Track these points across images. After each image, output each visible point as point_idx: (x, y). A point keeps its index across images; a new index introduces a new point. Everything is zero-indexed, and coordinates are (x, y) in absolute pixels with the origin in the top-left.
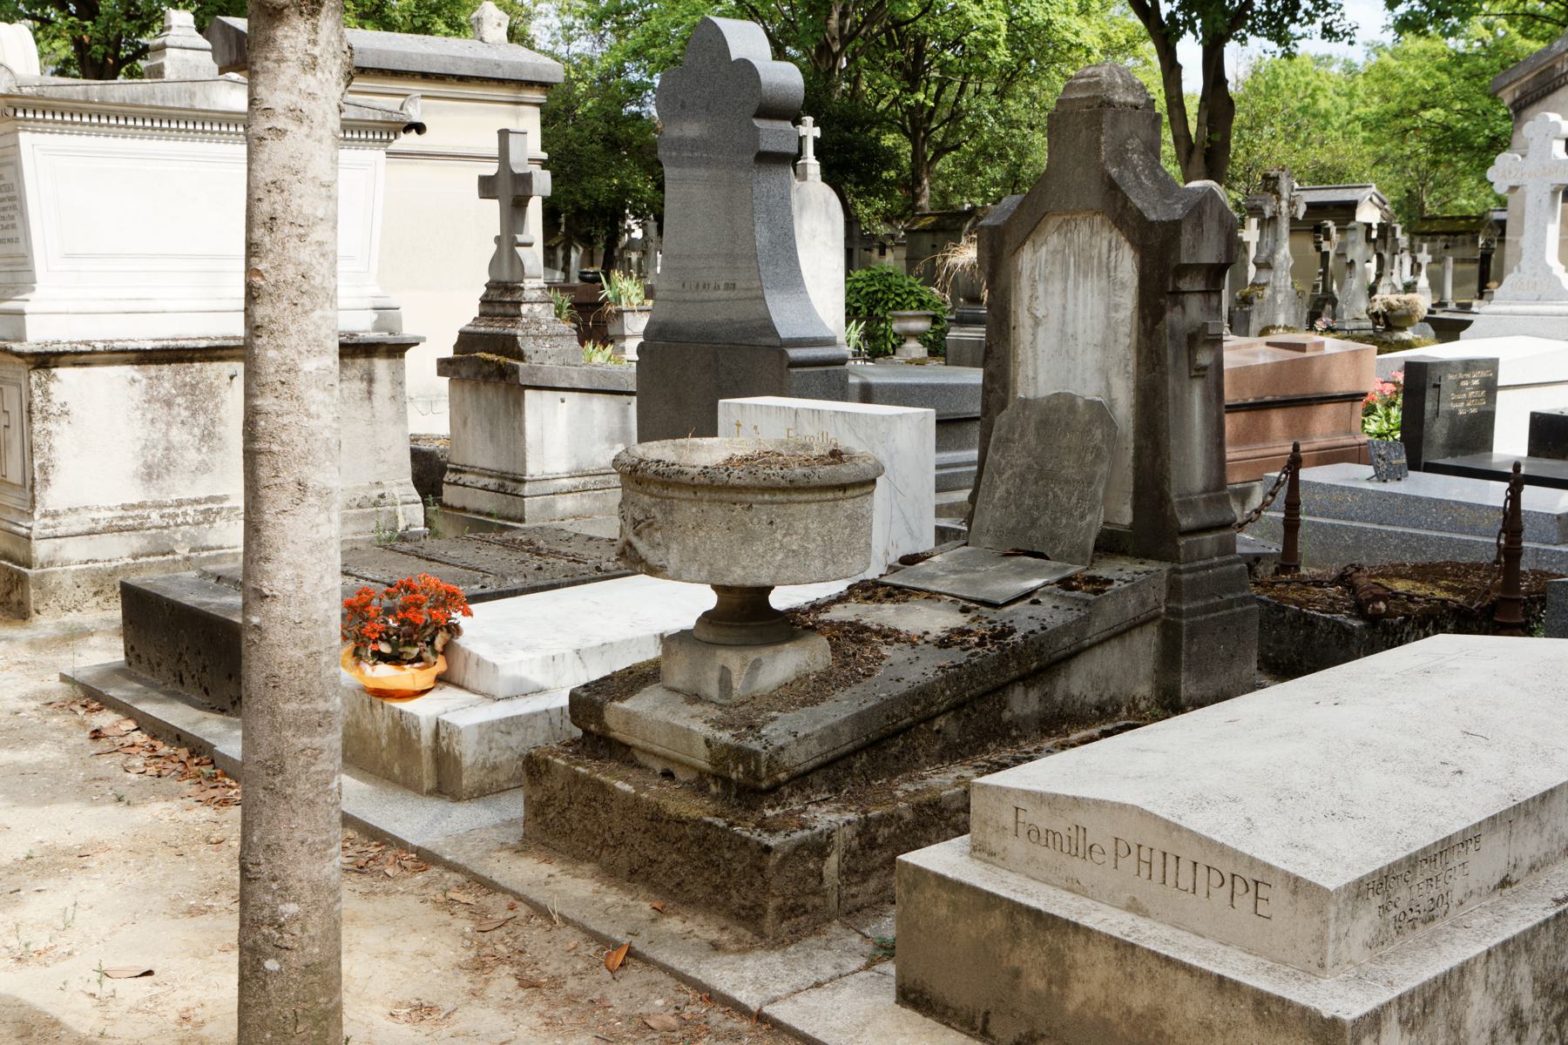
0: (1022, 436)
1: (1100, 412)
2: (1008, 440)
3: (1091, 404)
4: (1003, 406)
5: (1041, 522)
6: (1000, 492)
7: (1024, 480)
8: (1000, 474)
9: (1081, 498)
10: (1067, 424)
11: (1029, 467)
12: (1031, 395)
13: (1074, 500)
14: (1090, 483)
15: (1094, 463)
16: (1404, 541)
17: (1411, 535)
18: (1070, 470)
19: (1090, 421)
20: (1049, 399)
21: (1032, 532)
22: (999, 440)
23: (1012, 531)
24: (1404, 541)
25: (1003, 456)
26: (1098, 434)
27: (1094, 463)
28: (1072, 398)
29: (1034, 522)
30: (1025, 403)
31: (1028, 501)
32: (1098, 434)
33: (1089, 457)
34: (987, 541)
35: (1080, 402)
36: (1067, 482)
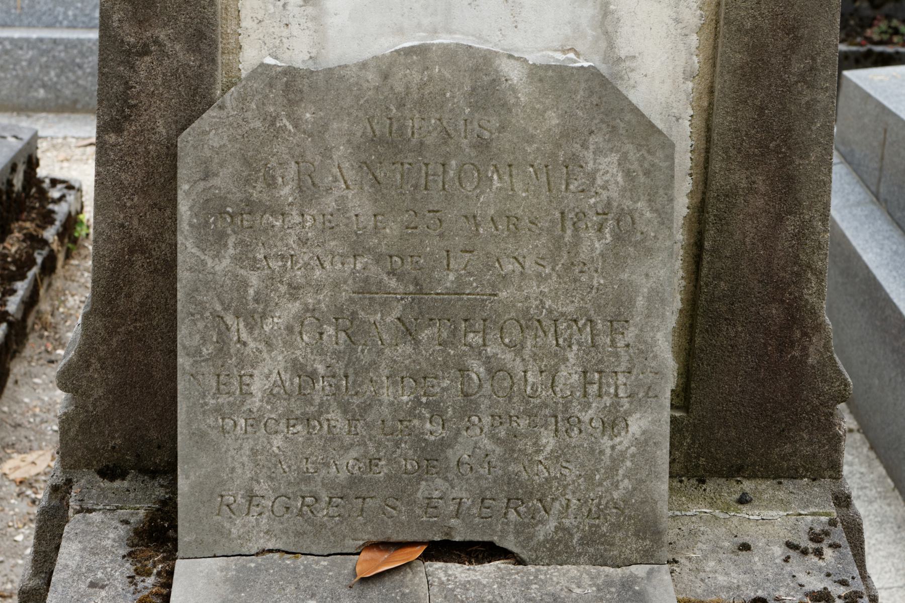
0: (309, 189)
1: (595, 97)
2: (251, 207)
3: (553, 78)
4: (196, 98)
5: (460, 451)
6: (267, 373)
7: (354, 329)
8: (253, 319)
9: (594, 371)
10: (482, 145)
11: (366, 288)
12: (298, 53)
13: (569, 375)
14: (618, 322)
15: (615, 257)
16: (43, 53)
17: (55, 41)
18: (530, 282)
19: (567, 134)
20: (386, 66)
21: (434, 487)
22: (212, 207)
23: (353, 489)
24: (43, 53)
25: (245, 258)
26: (608, 170)
27: (615, 257)
28: (480, 75)
29: (431, 457)
30: (290, 84)
31: (392, 395)
32: (608, 170)
33: (594, 245)
34: (254, 529)
35: (514, 73)
36: (528, 322)
